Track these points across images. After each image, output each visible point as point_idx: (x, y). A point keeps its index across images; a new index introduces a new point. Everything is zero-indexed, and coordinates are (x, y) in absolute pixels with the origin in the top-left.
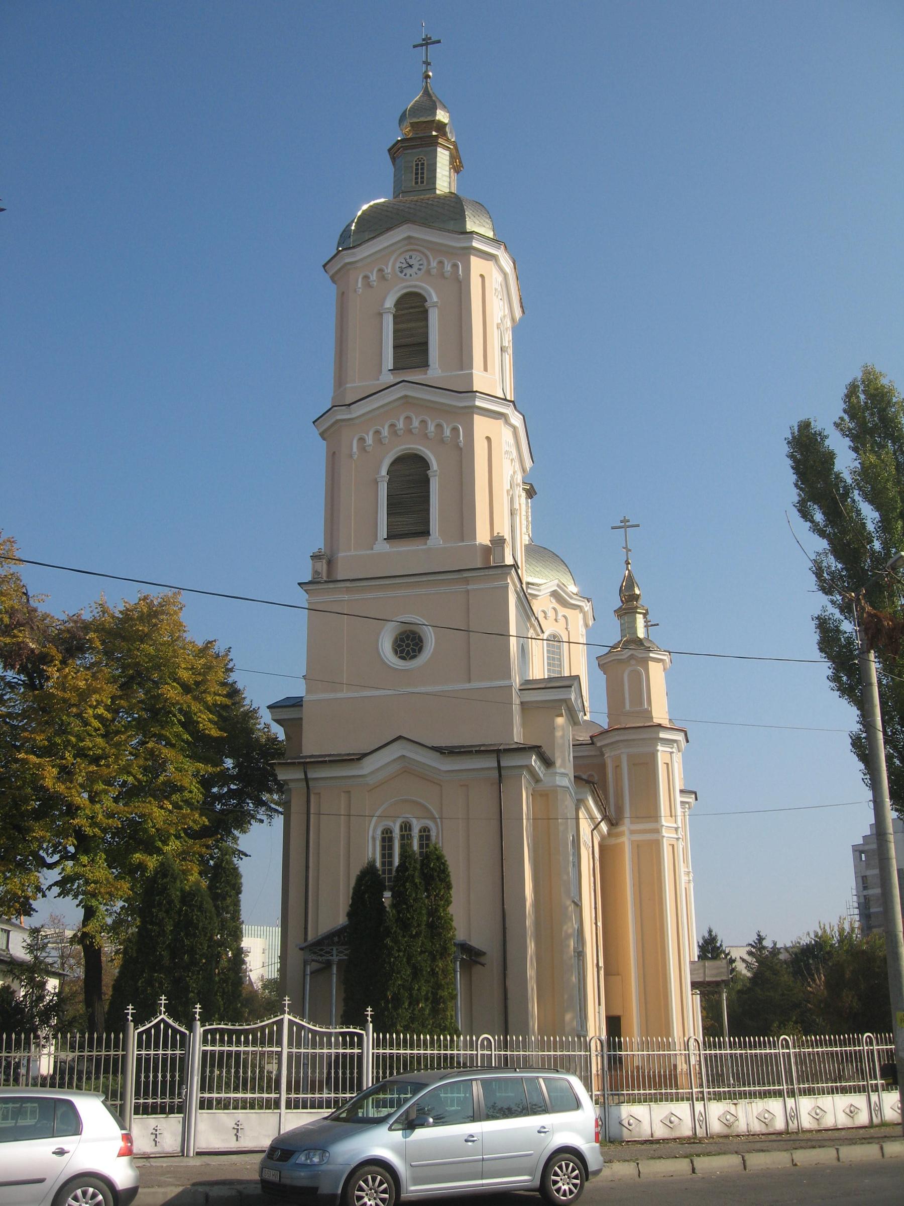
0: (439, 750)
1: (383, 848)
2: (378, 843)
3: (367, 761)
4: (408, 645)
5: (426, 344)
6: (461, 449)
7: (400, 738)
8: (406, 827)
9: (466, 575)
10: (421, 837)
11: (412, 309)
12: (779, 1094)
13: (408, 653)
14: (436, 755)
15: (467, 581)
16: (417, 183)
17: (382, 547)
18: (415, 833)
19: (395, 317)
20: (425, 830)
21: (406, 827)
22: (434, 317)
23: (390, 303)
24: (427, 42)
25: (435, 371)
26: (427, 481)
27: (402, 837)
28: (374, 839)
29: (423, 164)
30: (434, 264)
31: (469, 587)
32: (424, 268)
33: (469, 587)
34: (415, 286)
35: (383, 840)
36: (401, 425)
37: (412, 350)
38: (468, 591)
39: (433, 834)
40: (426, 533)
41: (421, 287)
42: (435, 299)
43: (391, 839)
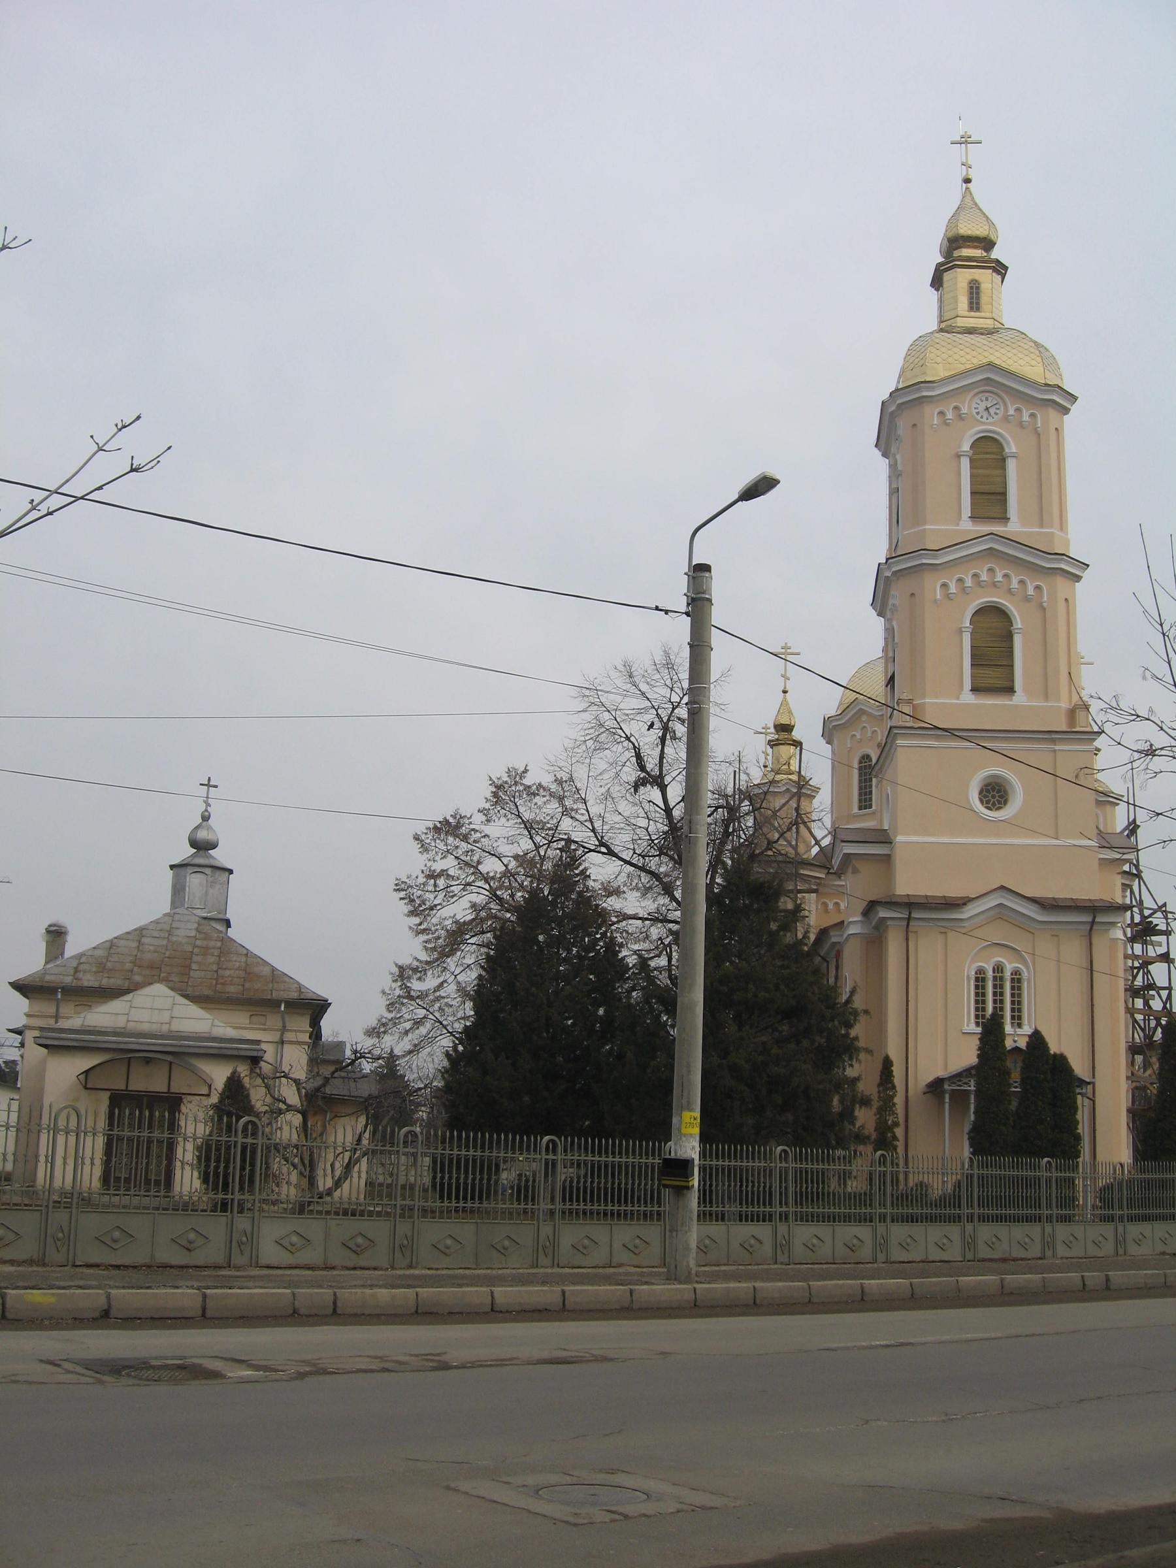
0: (1034, 900)
1: (977, 987)
2: (972, 983)
3: (970, 906)
4: (993, 797)
5: (1004, 494)
6: (1044, 609)
7: (1002, 888)
8: (998, 969)
9: (1054, 736)
10: (1013, 979)
11: (989, 454)
12: (766, 1218)
13: (994, 804)
14: (1034, 907)
15: (1054, 741)
16: (971, 309)
17: (968, 697)
18: (1007, 975)
19: (971, 461)
20: (1016, 972)
21: (998, 969)
22: (1012, 466)
23: (966, 447)
24: (965, 141)
25: (1014, 527)
26: (1009, 637)
27: (995, 978)
28: (969, 978)
29: (978, 288)
30: (1011, 412)
31: (1057, 747)
32: (1001, 412)
33: (1057, 747)
34: (998, 433)
35: (977, 979)
36: (984, 577)
37: (990, 500)
38: (1055, 751)
39: (1025, 974)
40: (1010, 690)
41: (1005, 439)
42: (1014, 450)
43: (984, 980)
